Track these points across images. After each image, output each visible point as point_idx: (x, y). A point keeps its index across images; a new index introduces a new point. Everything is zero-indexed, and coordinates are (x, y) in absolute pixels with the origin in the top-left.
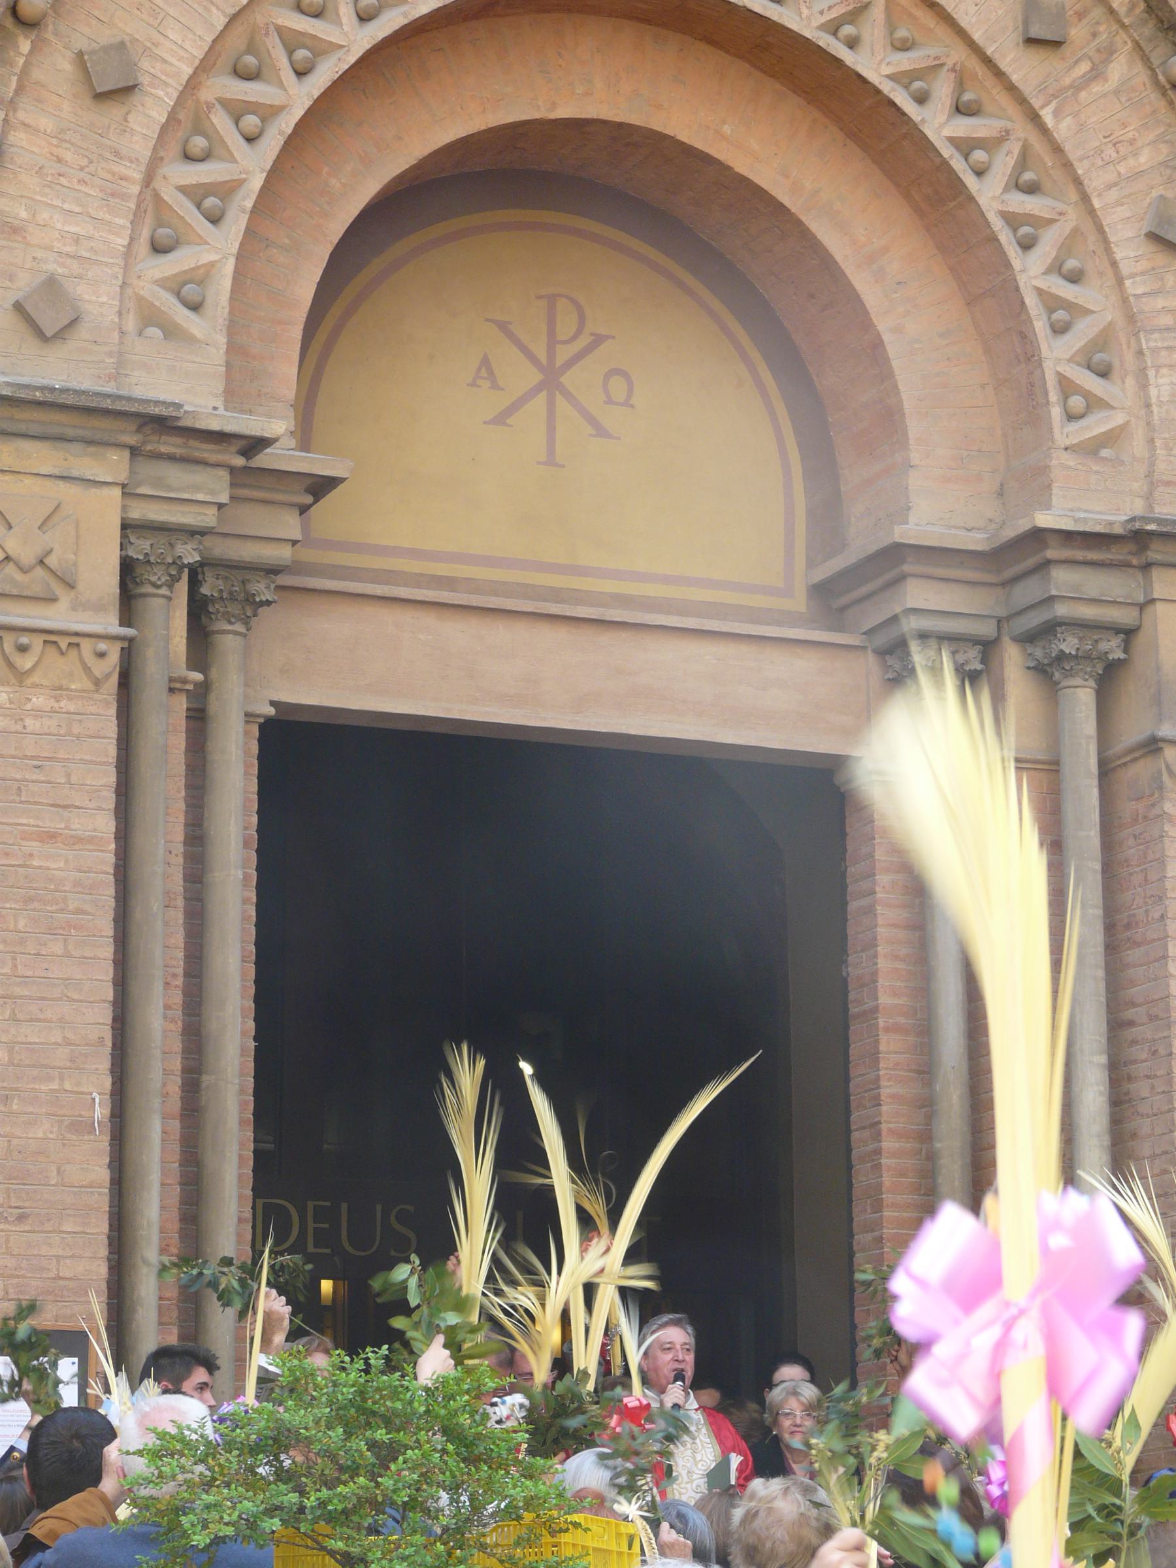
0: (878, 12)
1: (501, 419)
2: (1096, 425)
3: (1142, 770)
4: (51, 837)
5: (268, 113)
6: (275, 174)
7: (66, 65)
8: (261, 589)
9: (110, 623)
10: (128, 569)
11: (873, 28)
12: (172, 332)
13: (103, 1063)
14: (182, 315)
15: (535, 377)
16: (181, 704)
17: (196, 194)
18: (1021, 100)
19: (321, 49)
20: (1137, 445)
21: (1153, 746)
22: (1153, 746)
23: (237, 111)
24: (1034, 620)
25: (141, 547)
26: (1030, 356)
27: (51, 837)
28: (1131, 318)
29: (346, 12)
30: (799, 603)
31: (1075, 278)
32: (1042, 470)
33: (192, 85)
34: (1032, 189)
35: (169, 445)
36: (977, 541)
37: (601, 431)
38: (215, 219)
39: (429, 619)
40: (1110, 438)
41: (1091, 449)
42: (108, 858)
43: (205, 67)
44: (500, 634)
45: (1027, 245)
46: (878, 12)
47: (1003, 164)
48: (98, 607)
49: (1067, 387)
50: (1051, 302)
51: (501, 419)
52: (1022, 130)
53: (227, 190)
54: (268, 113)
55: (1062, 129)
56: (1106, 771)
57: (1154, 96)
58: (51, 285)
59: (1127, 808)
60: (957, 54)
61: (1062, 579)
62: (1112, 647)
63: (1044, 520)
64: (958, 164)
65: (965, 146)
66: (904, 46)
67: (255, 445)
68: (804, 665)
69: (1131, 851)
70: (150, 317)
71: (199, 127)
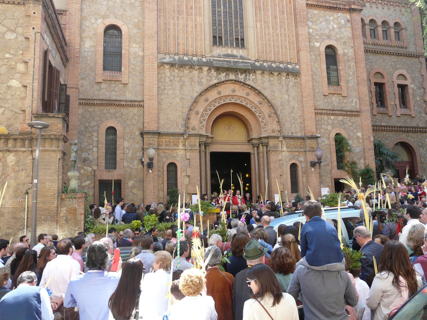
0: (249, 103)
1: (226, 131)
2: (265, 129)
3: (269, 152)
4: (195, 162)
5: (208, 114)
6: (208, 118)
7: (194, 112)
8: (209, 144)
9: (198, 148)
10: (200, 144)
11: (249, 104)
12: (202, 129)
13: (199, 176)
14: (203, 128)
15: (228, 128)
16: (204, 152)
17: (203, 119)
18: (259, 108)
19: (211, 109)
20: (268, 130)
21: (269, 151)
22: (269, 151)
23: (206, 114)
24: (261, 143)
25: (200, 143)
26: (260, 125)
27: (195, 162)
28: (267, 122)
29: (213, 107)
30: (247, 142)
31: (263, 119)
32: (261, 133)
33: (202, 112)
34: (260, 114)
35: (202, 136)
36: (257, 137)
37: (232, 131)
38: (204, 121)
39: (221, 145)
40: (266, 130)
41: (265, 131)
42: (199, 163)
43: (203, 111)
44: (226, 145)
45: (260, 117)
46: (249, 103)
47: (258, 112)
48: (198, 147)
49: (263, 127)
50: (262, 121)
51: (226, 131)
52: (259, 110)
53: (205, 119)
54: (208, 114)
55: (262, 109)
56: (267, 152)
57: (268, 107)
58: (194, 127)
59: (268, 155)
60: (255, 105)
61: (263, 140)
62: (267, 144)
63: (261, 136)
64: (255, 112)
65: (255, 111)
66: (251, 105)
67: (207, 136)
68: (247, 146)
69: (268, 158)
70: (200, 128)
71: (203, 115)
